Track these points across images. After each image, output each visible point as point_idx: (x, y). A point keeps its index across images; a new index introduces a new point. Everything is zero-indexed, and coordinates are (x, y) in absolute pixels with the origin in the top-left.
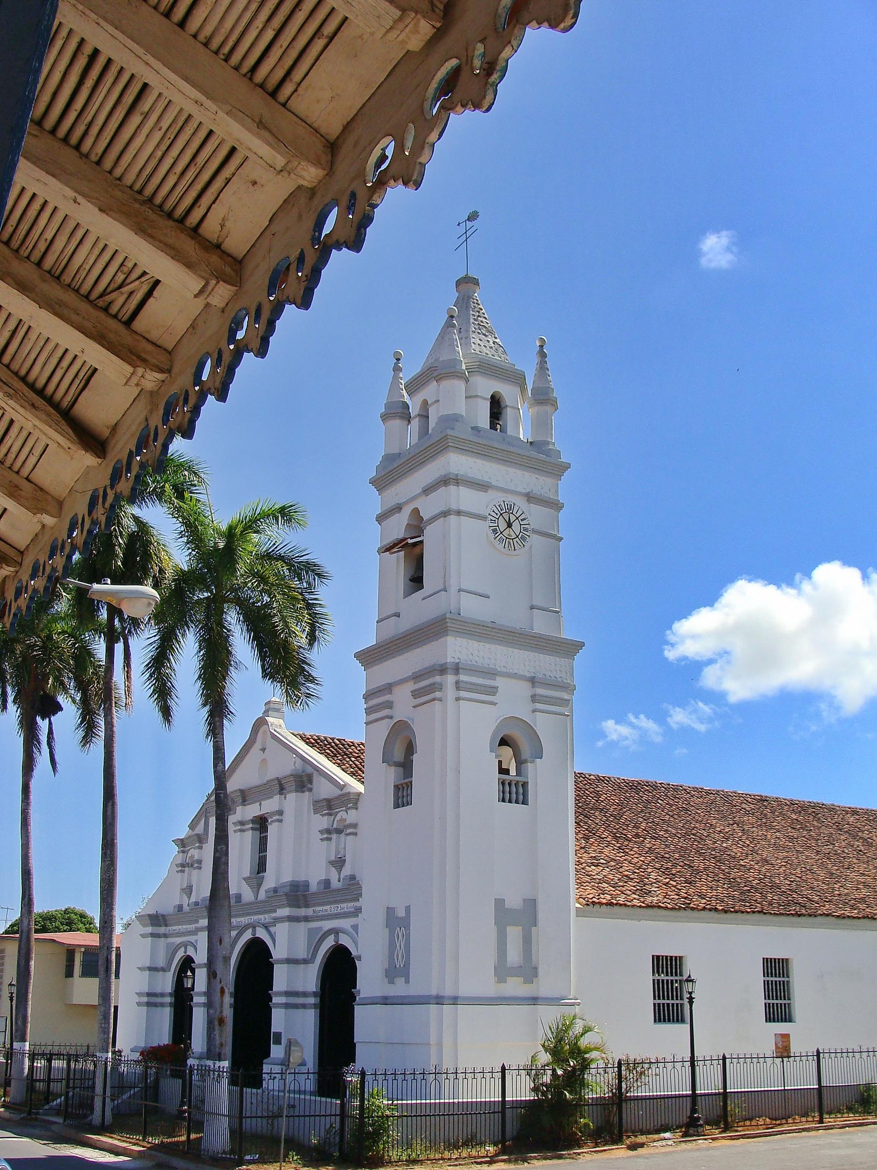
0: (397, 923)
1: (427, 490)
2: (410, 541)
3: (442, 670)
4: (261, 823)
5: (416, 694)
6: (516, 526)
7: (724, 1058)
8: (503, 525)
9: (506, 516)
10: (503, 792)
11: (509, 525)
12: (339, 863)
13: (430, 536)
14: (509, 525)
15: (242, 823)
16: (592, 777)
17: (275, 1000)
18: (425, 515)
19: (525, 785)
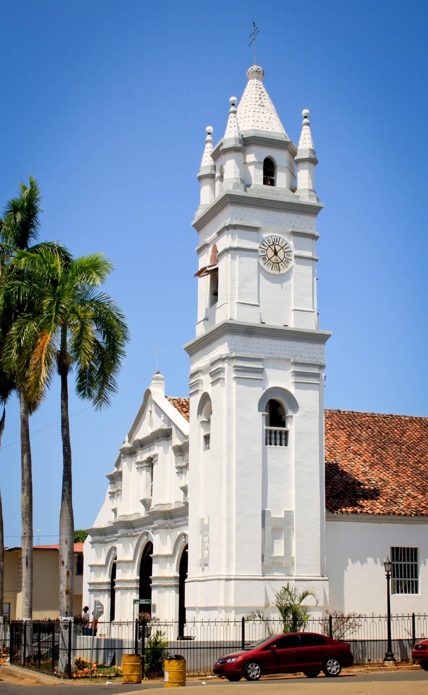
0: (205, 529)
1: (220, 233)
2: (208, 269)
3: (222, 360)
4: (150, 463)
5: (212, 375)
6: (281, 254)
7: (414, 616)
8: (270, 253)
9: (273, 247)
10: (270, 438)
11: (276, 253)
12: (185, 489)
13: (223, 266)
14: (276, 253)
15: (141, 463)
16: (407, 419)
17: (154, 583)
18: (220, 250)
19: (286, 433)
